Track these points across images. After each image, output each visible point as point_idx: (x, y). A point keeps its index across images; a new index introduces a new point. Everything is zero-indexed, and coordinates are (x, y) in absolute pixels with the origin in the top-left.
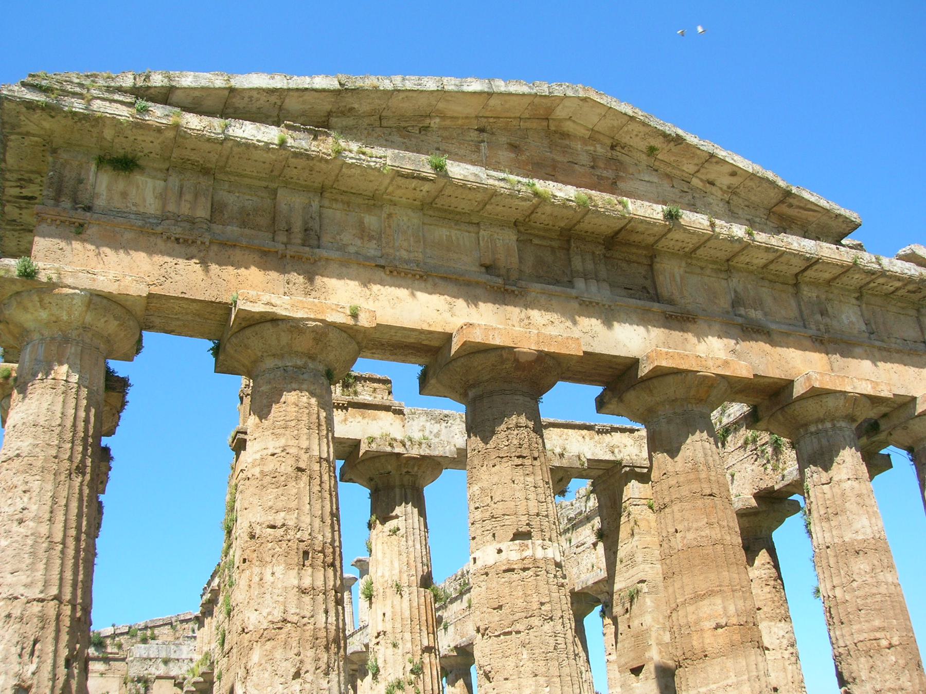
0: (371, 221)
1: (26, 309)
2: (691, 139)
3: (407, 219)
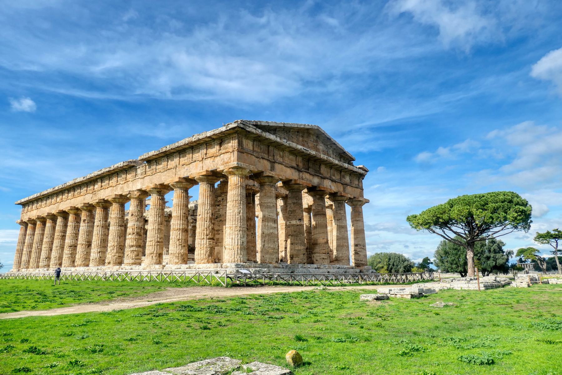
0: (281, 153)
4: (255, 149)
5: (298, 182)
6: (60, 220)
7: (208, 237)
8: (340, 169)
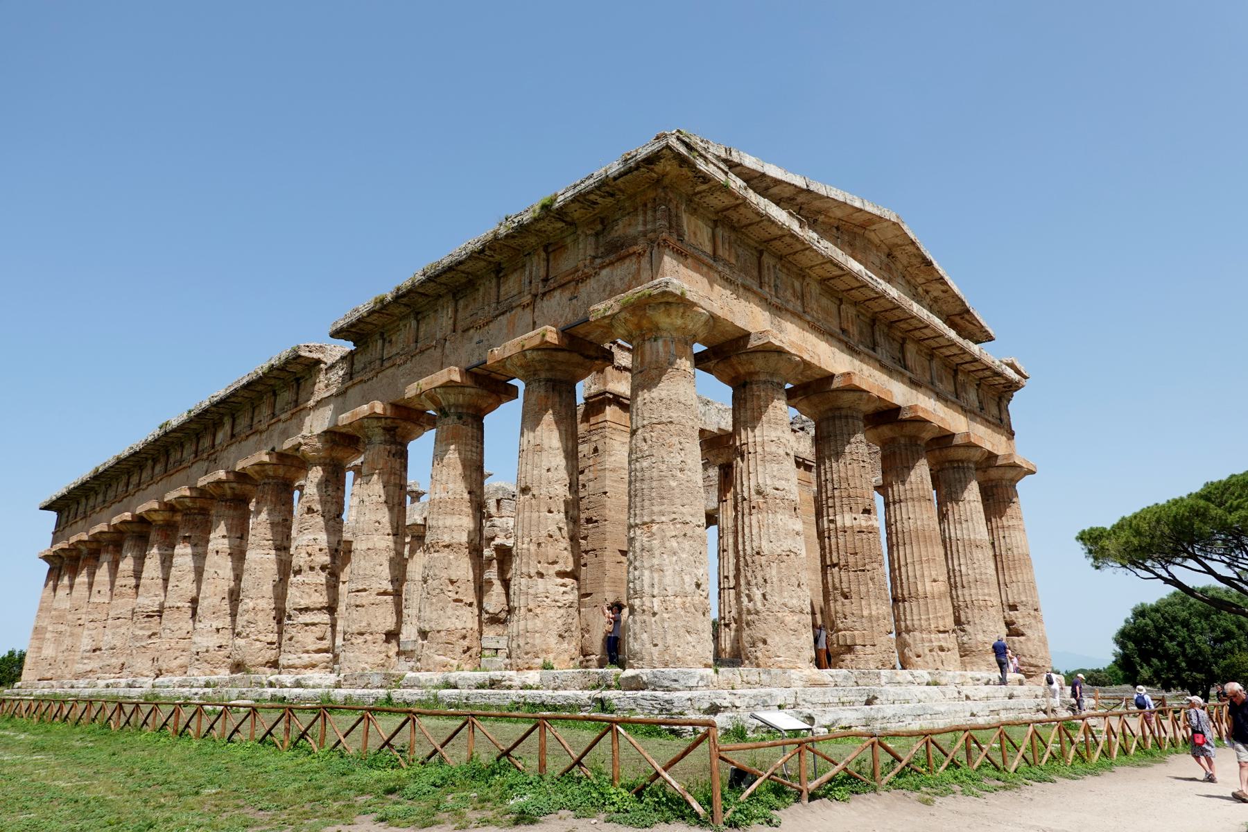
0: (797, 284)
1: (669, 315)
2: (936, 264)
3: (815, 288)
4: (720, 252)
5: (856, 381)
7: (557, 568)
8: (957, 360)
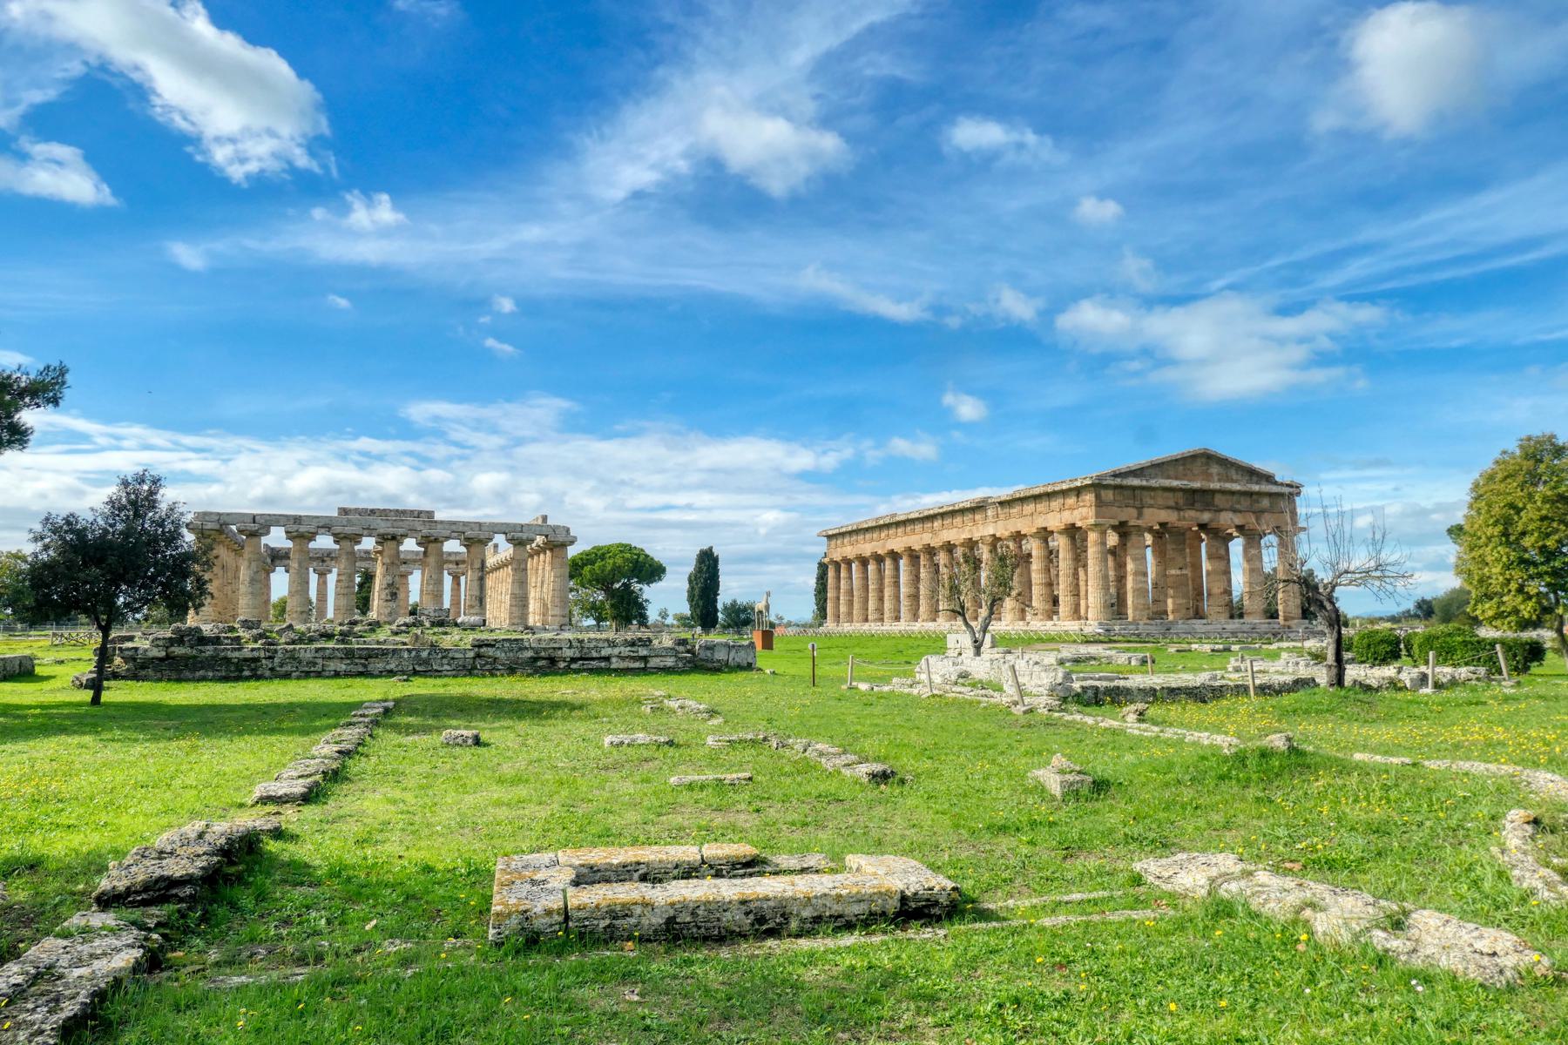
6: (888, 563)
